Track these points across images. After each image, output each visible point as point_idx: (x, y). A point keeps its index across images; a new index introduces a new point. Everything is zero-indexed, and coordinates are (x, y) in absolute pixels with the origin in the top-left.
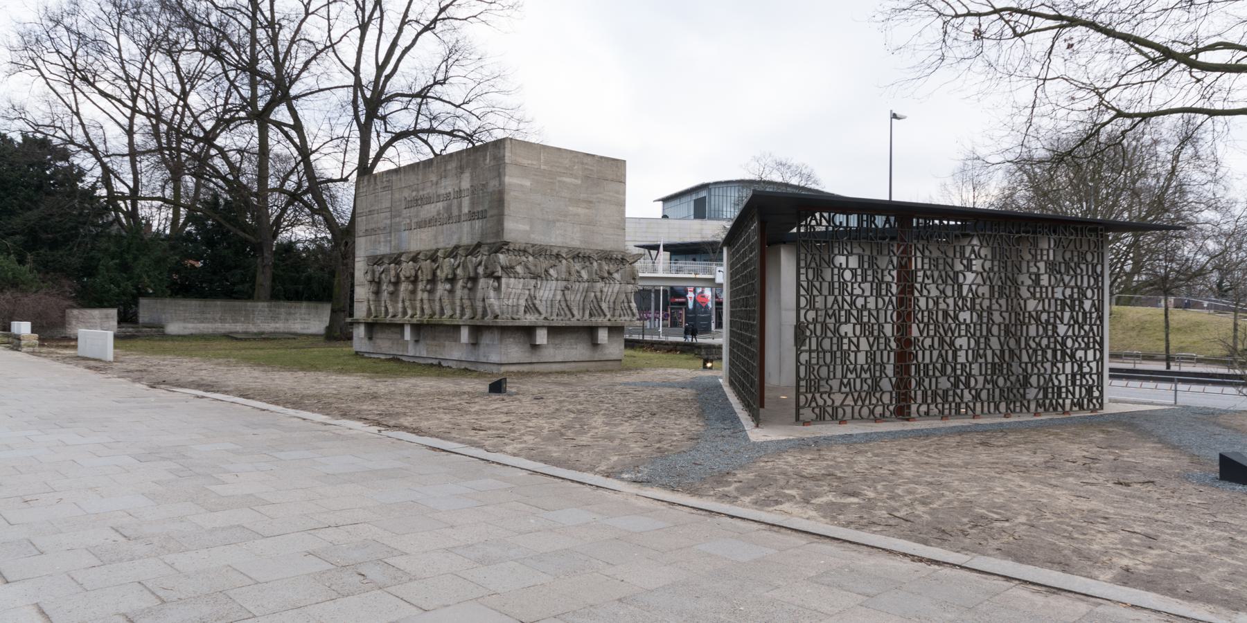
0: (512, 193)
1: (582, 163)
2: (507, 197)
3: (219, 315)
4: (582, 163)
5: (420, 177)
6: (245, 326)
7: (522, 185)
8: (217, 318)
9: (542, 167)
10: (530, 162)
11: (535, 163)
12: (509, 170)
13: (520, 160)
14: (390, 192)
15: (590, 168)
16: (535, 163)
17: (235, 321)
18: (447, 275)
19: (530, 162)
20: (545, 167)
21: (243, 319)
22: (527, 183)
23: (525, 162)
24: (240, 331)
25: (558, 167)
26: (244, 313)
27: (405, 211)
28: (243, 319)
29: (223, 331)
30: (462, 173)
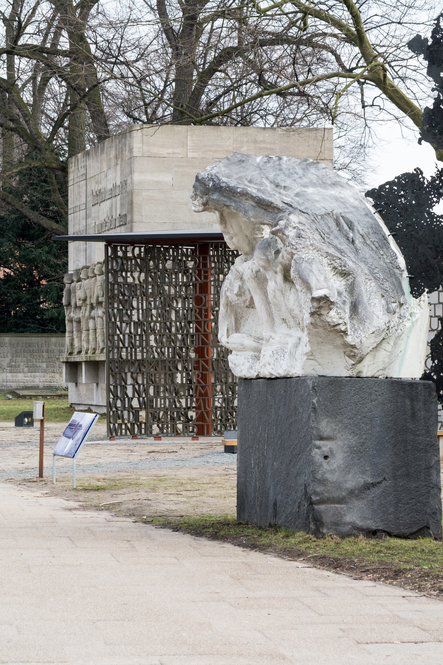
0: (144, 194)
1: (256, 142)
2: (136, 199)
3: (7, 360)
4: (256, 142)
5: (99, 165)
6: (48, 377)
7: (158, 183)
8: (5, 364)
9: (190, 155)
10: (170, 151)
11: (178, 150)
12: (137, 165)
13: (155, 150)
14: (85, 181)
15: (268, 146)
16: (178, 150)
17: (33, 369)
18: (98, 297)
19: (170, 151)
20: (196, 155)
21: (44, 365)
22: (167, 178)
23: (164, 152)
24: (41, 385)
25: (215, 152)
26: (45, 355)
27: (94, 209)
28: (44, 365)
29: (14, 385)
30: (117, 164)
